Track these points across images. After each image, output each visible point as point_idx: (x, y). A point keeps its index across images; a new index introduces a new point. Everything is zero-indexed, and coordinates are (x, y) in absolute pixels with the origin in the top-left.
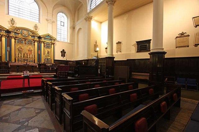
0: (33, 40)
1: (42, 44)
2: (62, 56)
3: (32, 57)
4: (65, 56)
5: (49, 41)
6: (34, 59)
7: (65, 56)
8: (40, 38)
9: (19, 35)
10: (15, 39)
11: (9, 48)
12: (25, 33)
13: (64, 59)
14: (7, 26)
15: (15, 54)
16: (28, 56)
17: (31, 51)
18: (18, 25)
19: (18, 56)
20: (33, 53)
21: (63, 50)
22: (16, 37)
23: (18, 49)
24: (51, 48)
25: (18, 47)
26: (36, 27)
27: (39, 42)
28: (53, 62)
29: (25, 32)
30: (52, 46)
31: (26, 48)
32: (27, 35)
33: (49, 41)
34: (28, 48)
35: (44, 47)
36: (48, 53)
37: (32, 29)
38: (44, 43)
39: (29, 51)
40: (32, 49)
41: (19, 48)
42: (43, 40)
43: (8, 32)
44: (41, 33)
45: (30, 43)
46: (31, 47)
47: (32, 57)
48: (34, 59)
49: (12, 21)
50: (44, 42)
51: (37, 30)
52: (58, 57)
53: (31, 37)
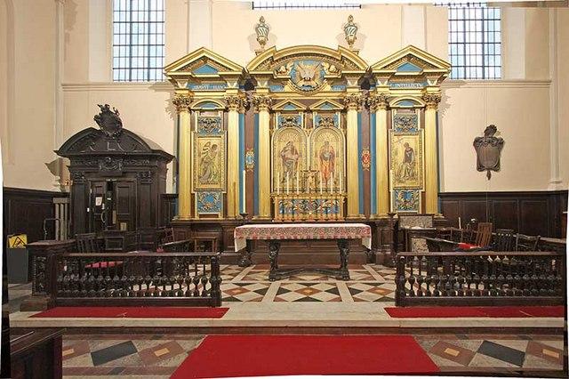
0: (341, 101)
1: (381, 115)
2: (480, 168)
3: (336, 190)
4: (497, 168)
5: (415, 93)
6: (346, 200)
7: (497, 168)
8: (368, 80)
9: (287, 88)
10: (271, 112)
11: (250, 155)
12: (307, 76)
13: (499, 183)
14: (242, 56)
15: (272, 181)
16: (321, 186)
17: (332, 156)
18: (283, 40)
19: (283, 190)
20: (338, 169)
21: (491, 130)
22: (275, 102)
23: (283, 157)
24: (423, 126)
25: (283, 145)
26: (351, 28)
27: (367, 107)
28: (432, 206)
29: (308, 69)
30: (430, 114)
31: (311, 143)
32: (313, 83)
33: (415, 93)
34: (318, 147)
35: (389, 126)
36: (408, 159)
37: (330, 40)
38: (388, 108)
39: (323, 158)
40: (336, 146)
41: (285, 150)
42: (383, 87)
43: (247, 82)
44: (373, 54)
45: (331, 116)
46: (330, 139)
47: (336, 190)
48: (346, 200)
49: (262, 29)
50: (387, 100)
51: (355, 46)
52: (462, 176)
53: (328, 88)
